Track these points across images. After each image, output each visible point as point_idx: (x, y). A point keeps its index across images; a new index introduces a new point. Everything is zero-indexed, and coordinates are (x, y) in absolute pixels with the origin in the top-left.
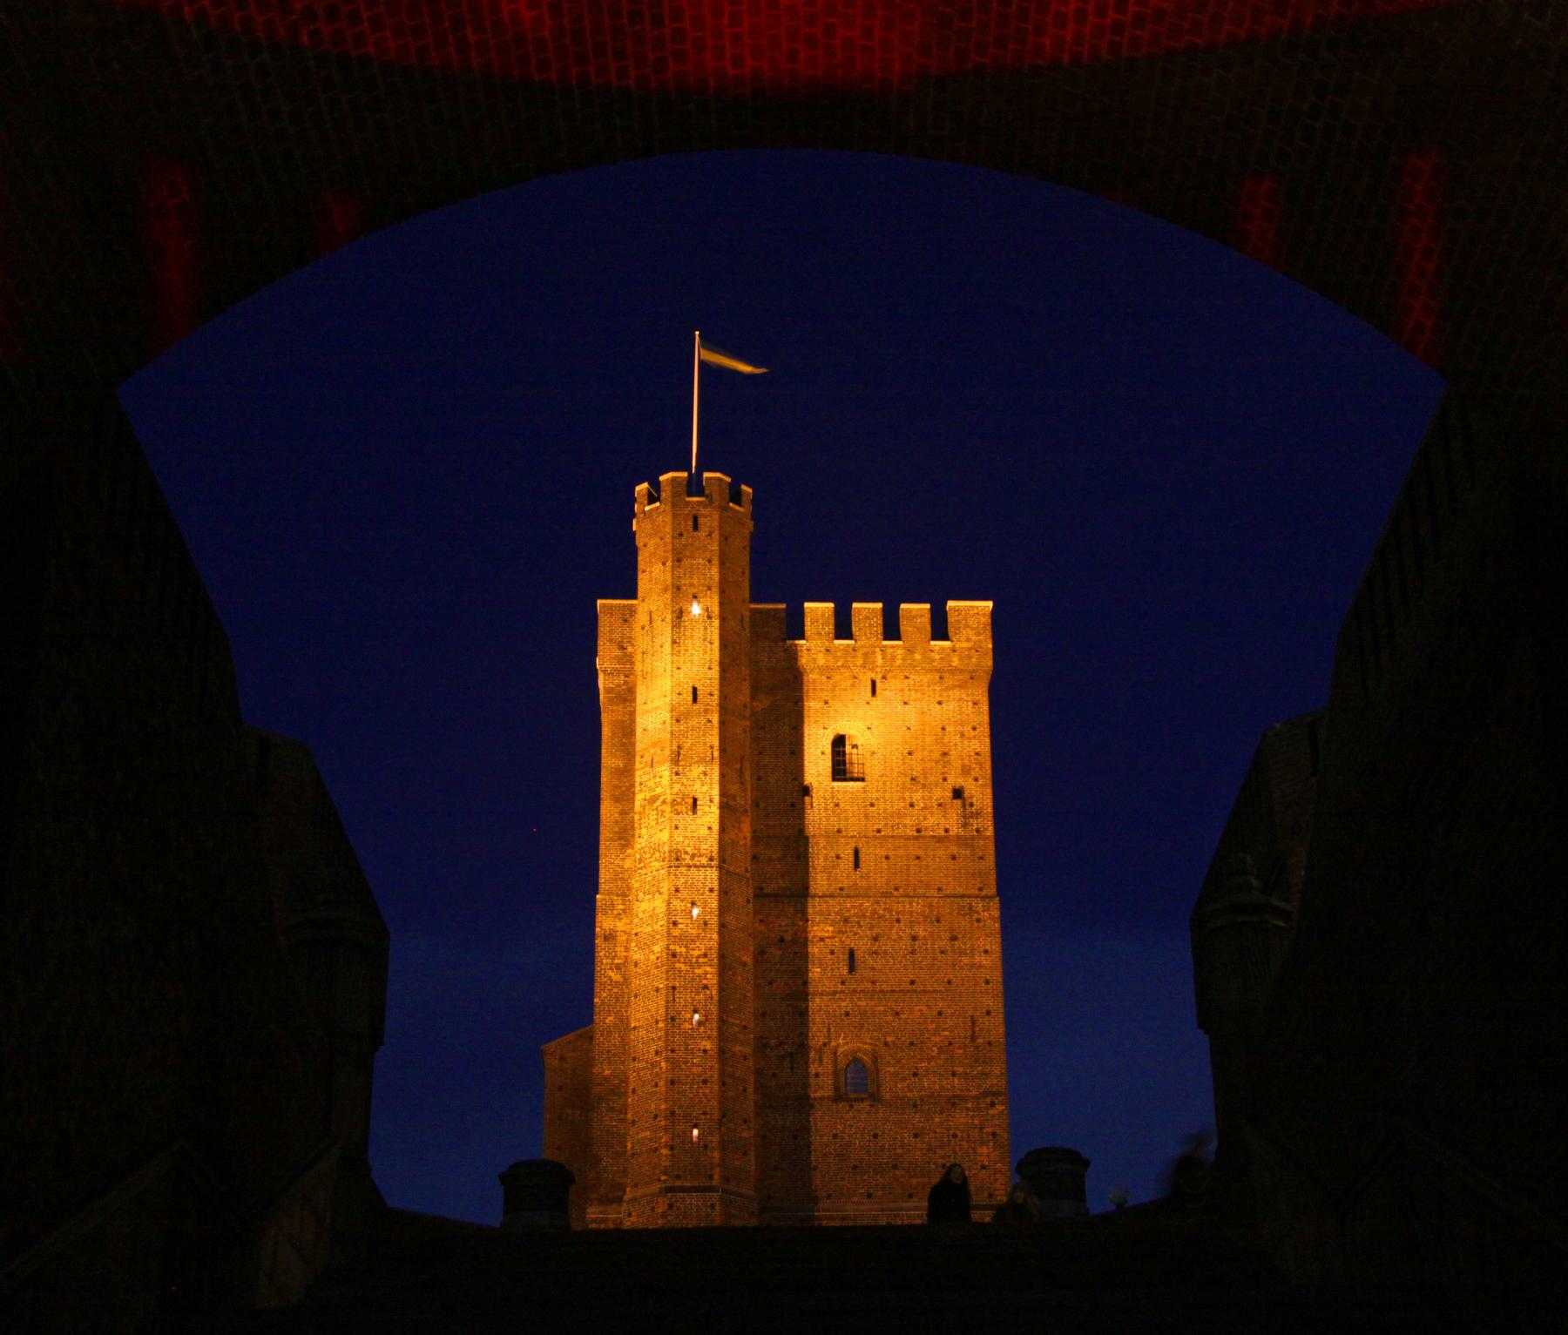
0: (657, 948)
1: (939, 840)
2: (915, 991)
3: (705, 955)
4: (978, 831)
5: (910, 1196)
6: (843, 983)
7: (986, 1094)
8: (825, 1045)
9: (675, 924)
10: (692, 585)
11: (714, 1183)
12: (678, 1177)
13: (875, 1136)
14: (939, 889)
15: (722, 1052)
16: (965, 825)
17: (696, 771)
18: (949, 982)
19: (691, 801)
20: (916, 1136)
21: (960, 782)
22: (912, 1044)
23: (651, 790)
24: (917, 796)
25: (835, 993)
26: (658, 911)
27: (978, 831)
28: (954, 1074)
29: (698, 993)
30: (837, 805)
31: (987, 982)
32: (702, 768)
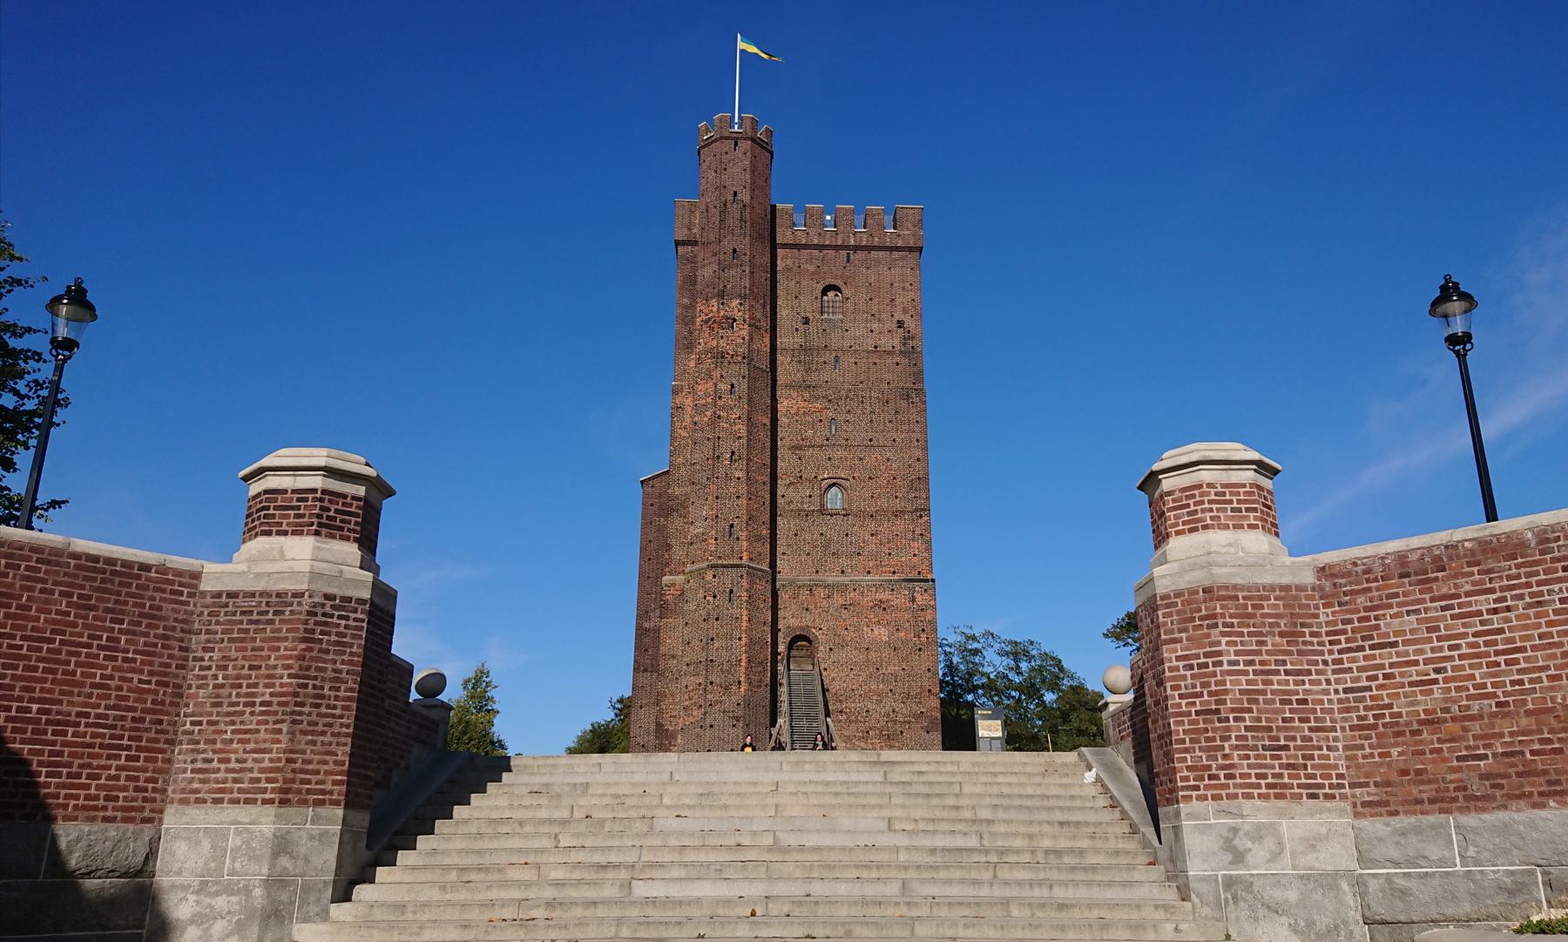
0: (708, 414)
1: (889, 353)
2: (873, 446)
3: (739, 418)
4: (913, 347)
5: (869, 572)
6: (827, 440)
7: (916, 510)
8: (816, 477)
9: (720, 398)
10: (733, 185)
11: (743, 562)
12: (720, 557)
13: (847, 535)
14: (888, 383)
15: (749, 479)
16: (905, 344)
17: (736, 302)
18: (894, 440)
19: (731, 321)
20: (872, 535)
21: (902, 318)
22: (870, 478)
23: (706, 315)
24: (875, 326)
25: (822, 446)
26: (709, 390)
27: (913, 347)
28: (896, 497)
29: (734, 442)
30: (824, 330)
31: (918, 440)
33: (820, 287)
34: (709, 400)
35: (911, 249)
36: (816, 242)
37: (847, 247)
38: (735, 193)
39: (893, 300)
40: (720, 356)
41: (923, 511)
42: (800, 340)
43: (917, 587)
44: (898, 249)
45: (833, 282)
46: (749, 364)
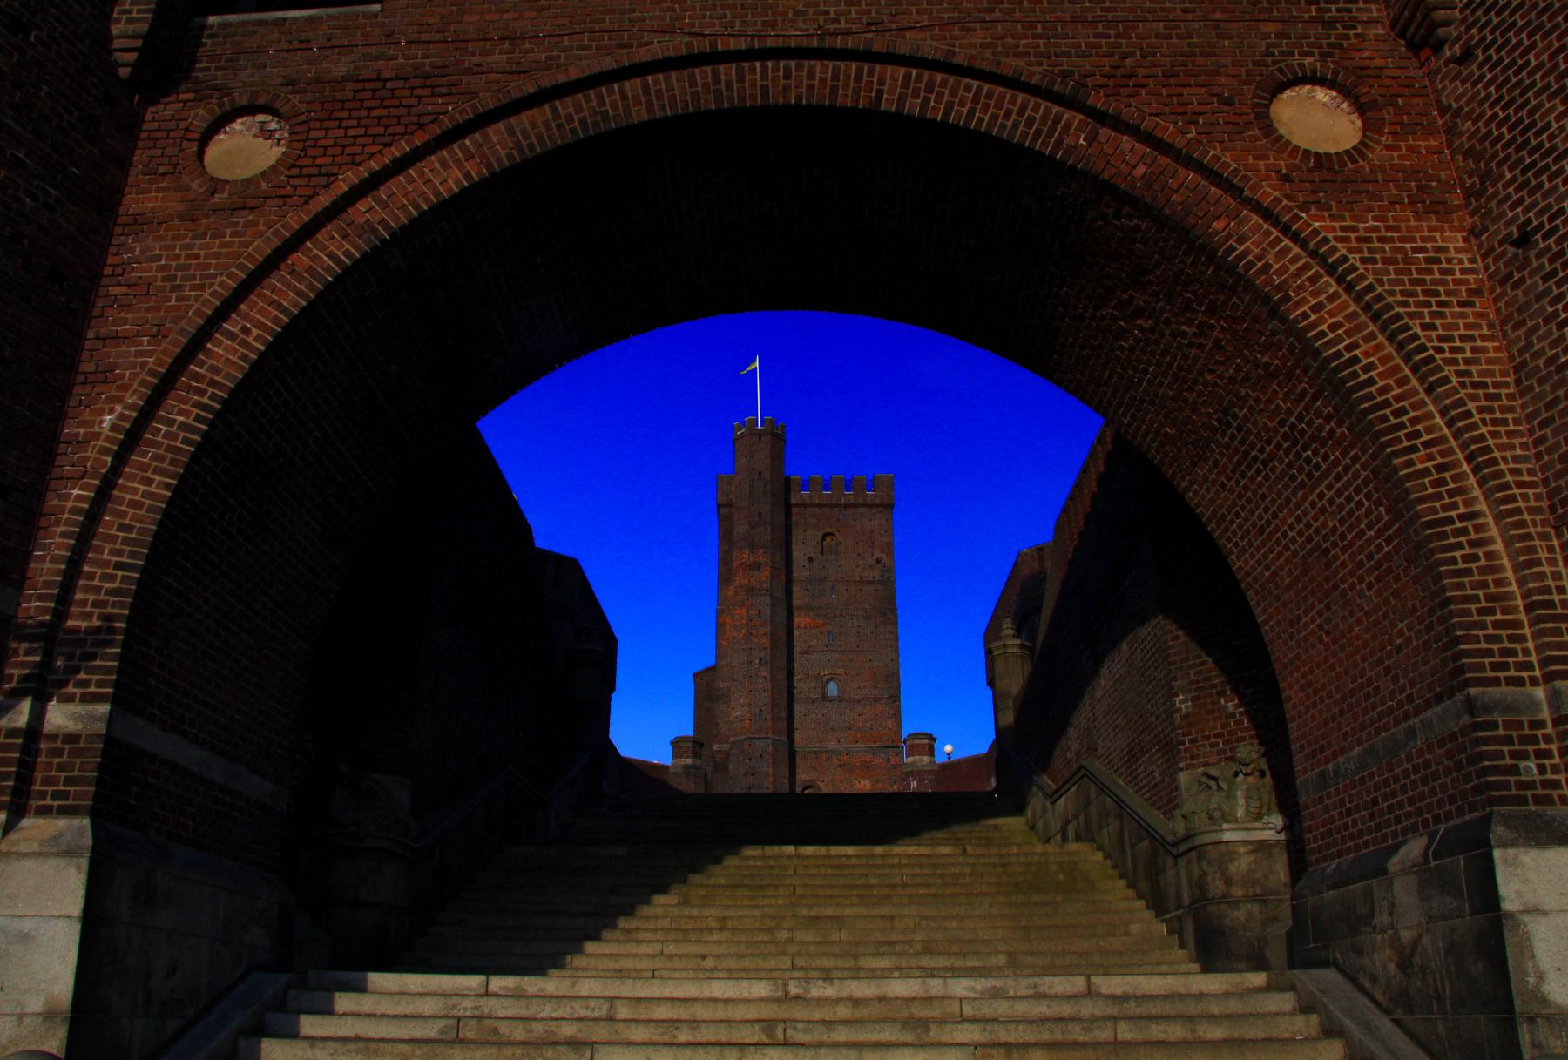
1: (871, 582)
7: (891, 697)
11: (770, 735)
15: (772, 677)
21: (880, 556)
32: (762, 551)
33: (820, 534)
34: (744, 621)
35: (885, 506)
36: (817, 502)
37: (840, 505)
38: (760, 473)
39: (873, 543)
40: (750, 590)
41: (895, 698)
42: (806, 574)
43: (891, 752)
44: (877, 506)
45: (830, 530)
46: (771, 596)
